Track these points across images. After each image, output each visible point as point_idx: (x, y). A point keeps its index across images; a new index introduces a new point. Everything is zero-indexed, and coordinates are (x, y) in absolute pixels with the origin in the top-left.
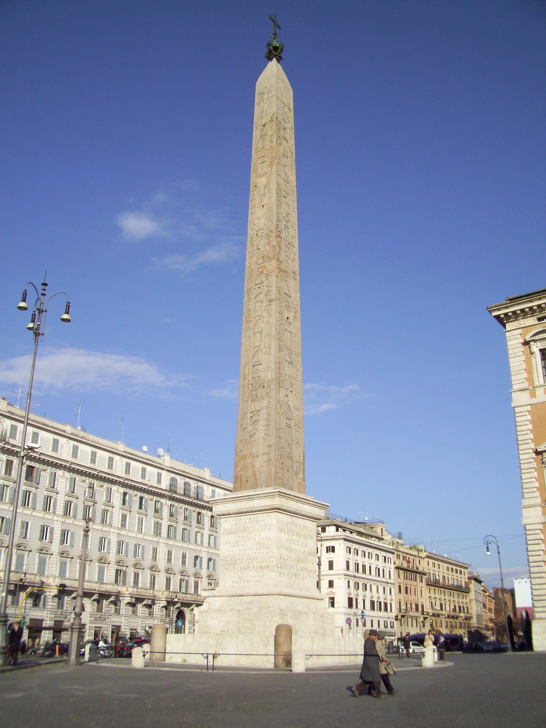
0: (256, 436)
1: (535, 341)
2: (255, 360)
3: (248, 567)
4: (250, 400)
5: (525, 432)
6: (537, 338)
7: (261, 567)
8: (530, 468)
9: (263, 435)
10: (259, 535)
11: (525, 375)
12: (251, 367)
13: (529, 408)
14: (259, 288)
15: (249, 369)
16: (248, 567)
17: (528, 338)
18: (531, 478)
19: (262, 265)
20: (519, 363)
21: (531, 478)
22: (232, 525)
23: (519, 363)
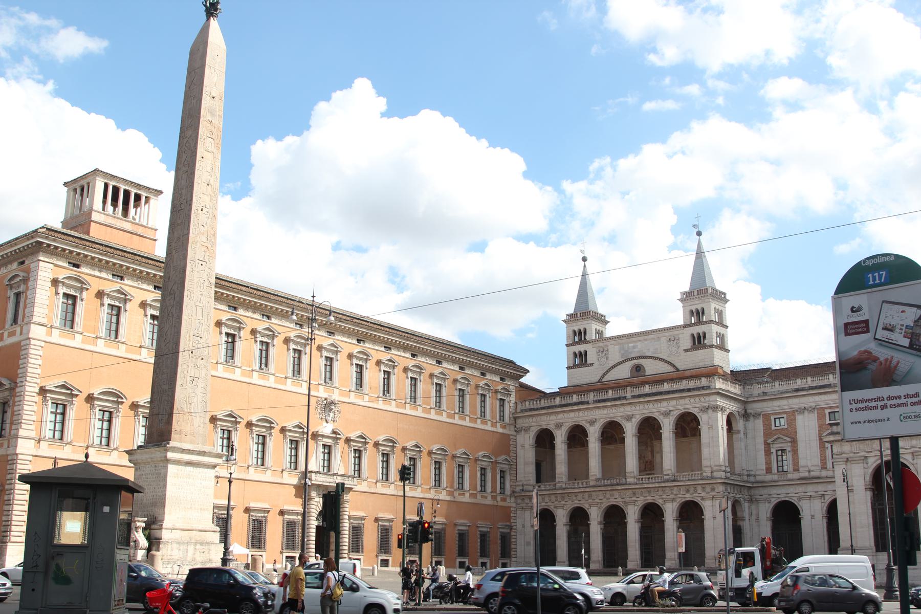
0: (195, 400)
1: (63, 283)
2: (196, 331)
3: (191, 508)
4: (190, 366)
5: (35, 366)
6: (66, 281)
7: (201, 509)
8: (32, 402)
9: (201, 401)
10: (201, 484)
11: (46, 311)
12: (192, 335)
13: (43, 344)
14: (202, 265)
15: (190, 336)
16: (191, 508)
17: (61, 278)
18: (31, 411)
19: (206, 244)
20: (44, 297)
21: (31, 411)
22: (178, 470)
23: (44, 297)
